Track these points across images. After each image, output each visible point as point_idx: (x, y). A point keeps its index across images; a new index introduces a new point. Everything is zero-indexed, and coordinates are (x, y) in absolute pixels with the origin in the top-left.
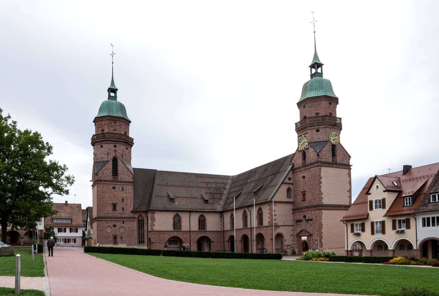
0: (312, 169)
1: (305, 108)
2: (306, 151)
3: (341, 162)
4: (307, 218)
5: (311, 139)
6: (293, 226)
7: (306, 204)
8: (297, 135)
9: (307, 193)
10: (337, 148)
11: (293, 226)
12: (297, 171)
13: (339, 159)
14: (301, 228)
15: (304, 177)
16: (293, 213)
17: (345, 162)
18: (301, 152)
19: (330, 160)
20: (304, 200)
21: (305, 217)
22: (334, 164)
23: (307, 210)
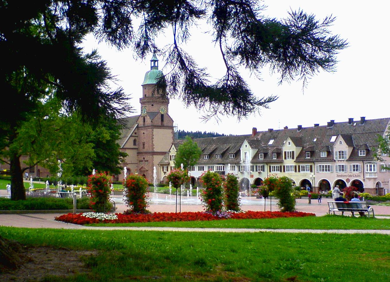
0: (148, 129)
1: (146, 90)
2: (145, 117)
3: (167, 125)
4: (145, 159)
5: (148, 110)
6: (137, 164)
7: (145, 150)
8: (141, 106)
9: (145, 144)
10: (165, 117)
11: (137, 164)
12: (140, 129)
13: (165, 123)
14: (142, 166)
15: (144, 133)
16: (138, 155)
17: (170, 125)
18: (143, 117)
19: (160, 124)
20: (144, 148)
21: (144, 158)
22: (162, 127)
23: (145, 154)
